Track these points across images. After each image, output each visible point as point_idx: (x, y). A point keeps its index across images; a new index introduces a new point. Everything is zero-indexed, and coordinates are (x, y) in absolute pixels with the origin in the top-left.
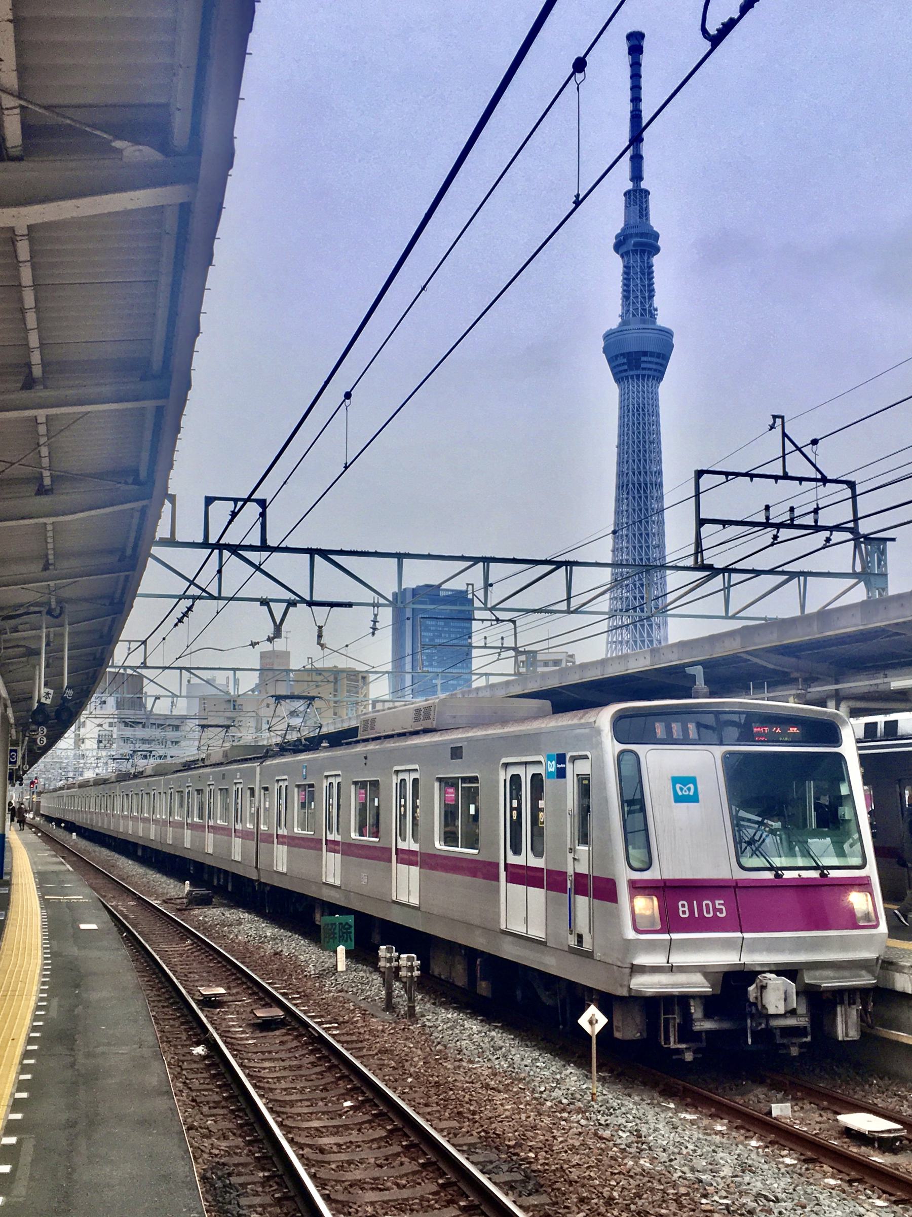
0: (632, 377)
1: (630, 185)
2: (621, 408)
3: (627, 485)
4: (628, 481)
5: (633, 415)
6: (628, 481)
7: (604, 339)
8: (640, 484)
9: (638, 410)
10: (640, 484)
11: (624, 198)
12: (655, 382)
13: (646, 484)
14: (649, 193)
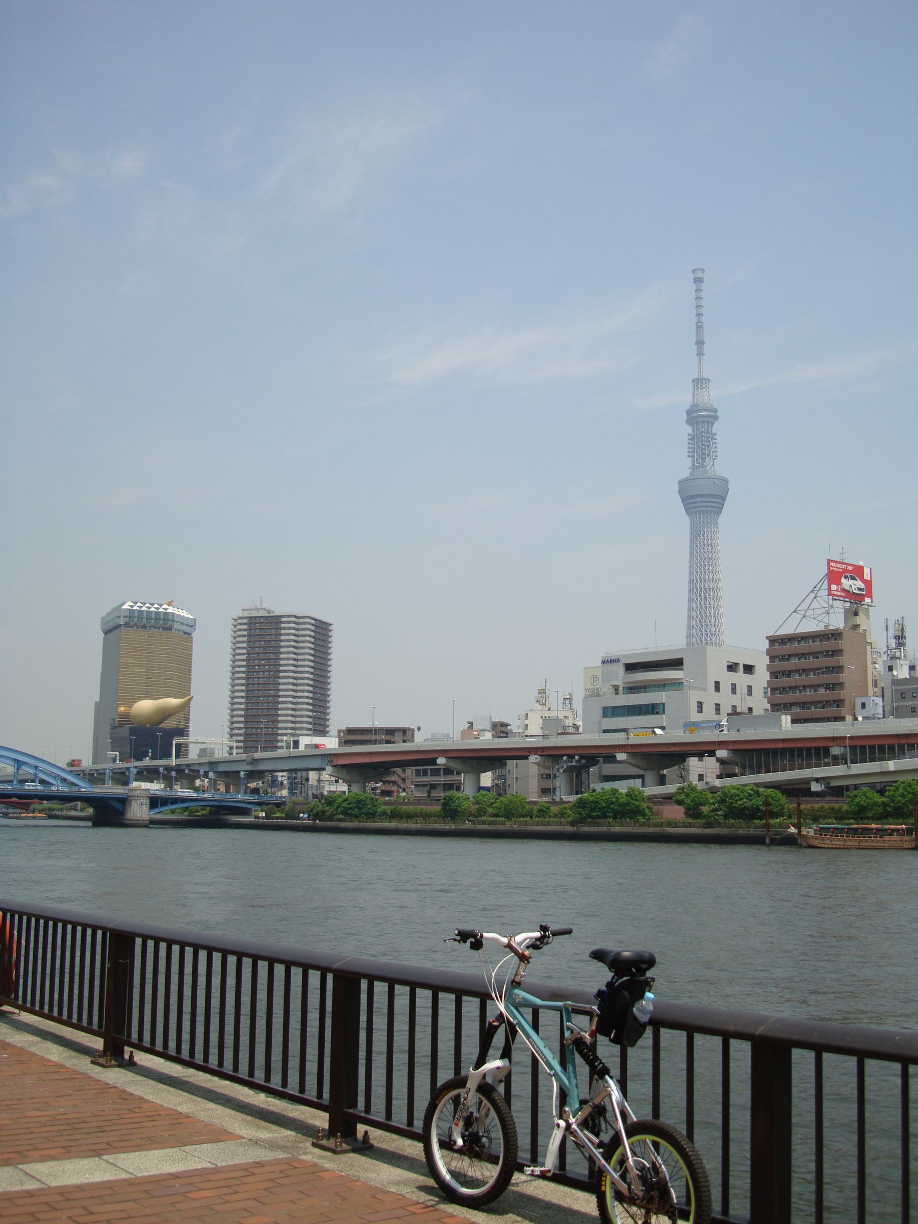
0: (695, 512)
1: (696, 377)
4: (693, 587)
6: (693, 587)
10: (701, 590)
12: (715, 515)
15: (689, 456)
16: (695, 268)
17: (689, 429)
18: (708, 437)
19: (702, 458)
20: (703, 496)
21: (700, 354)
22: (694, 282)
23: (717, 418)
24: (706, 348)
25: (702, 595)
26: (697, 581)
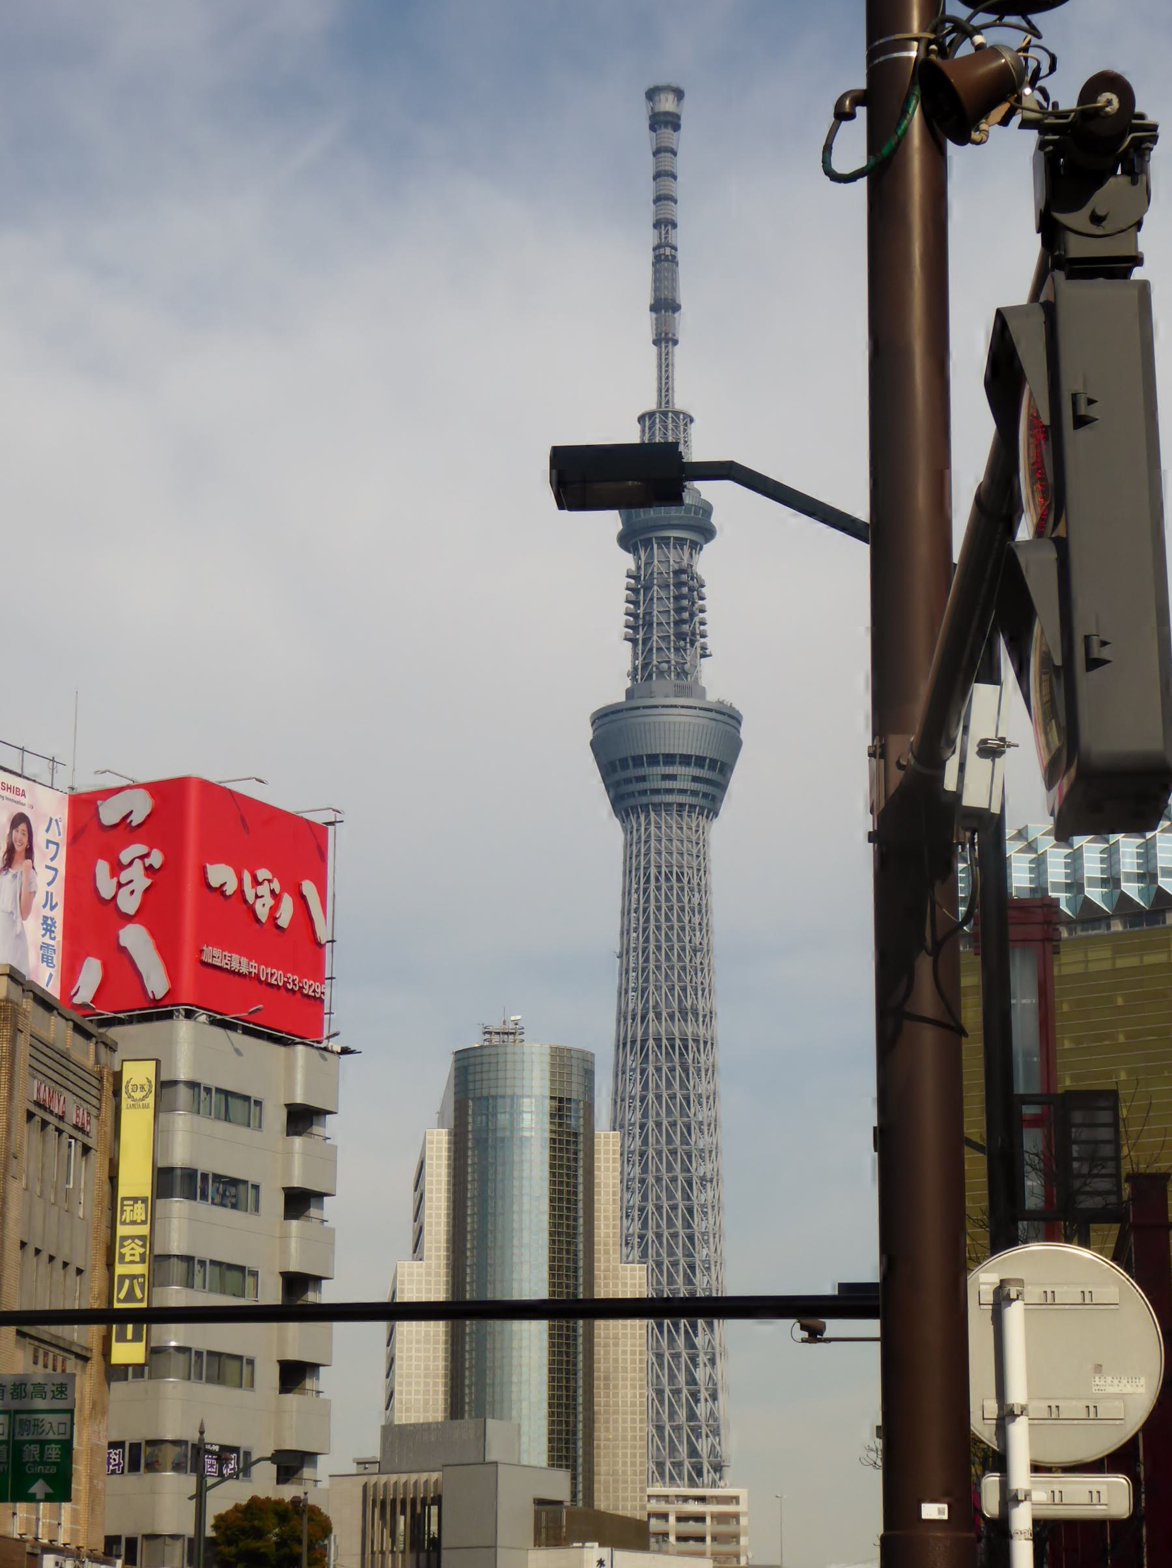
1: (651, 405)
2: (627, 872)
3: (644, 1041)
4: (646, 1032)
5: (658, 889)
6: (646, 1032)
7: (592, 725)
8: (671, 1040)
9: (668, 879)
10: (671, 1040)
11: (638, 427)
13: (684, 1041)
14: (692, 421)
15: (626, 639)
16: (662, 82)
17: (627, 561)
18: (691, 590)
19: (677, 649)
20: (686, 760)
21: (664, 339)
22: (653, 128)
23: (708, 533)
24: (686, 323)
25: (676, 1058)
26: (658, 1016)
